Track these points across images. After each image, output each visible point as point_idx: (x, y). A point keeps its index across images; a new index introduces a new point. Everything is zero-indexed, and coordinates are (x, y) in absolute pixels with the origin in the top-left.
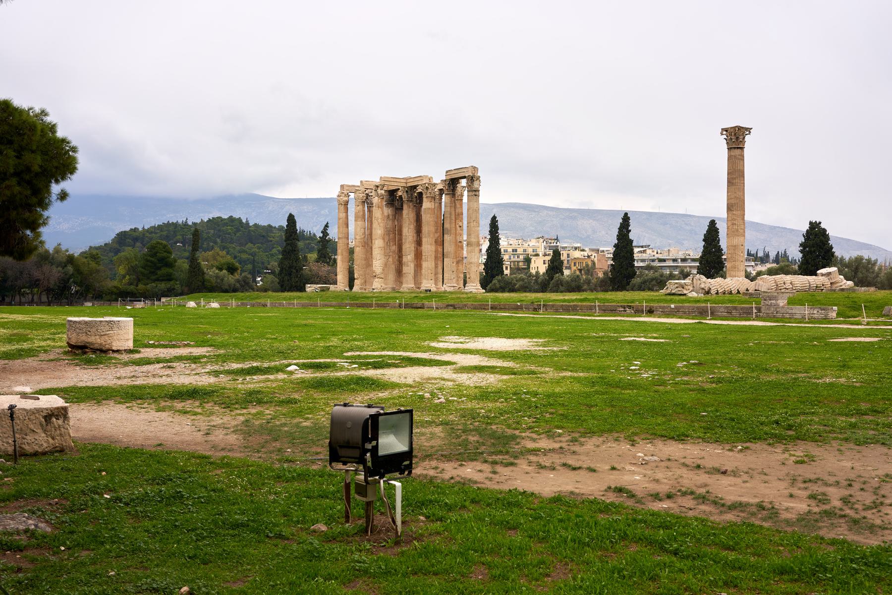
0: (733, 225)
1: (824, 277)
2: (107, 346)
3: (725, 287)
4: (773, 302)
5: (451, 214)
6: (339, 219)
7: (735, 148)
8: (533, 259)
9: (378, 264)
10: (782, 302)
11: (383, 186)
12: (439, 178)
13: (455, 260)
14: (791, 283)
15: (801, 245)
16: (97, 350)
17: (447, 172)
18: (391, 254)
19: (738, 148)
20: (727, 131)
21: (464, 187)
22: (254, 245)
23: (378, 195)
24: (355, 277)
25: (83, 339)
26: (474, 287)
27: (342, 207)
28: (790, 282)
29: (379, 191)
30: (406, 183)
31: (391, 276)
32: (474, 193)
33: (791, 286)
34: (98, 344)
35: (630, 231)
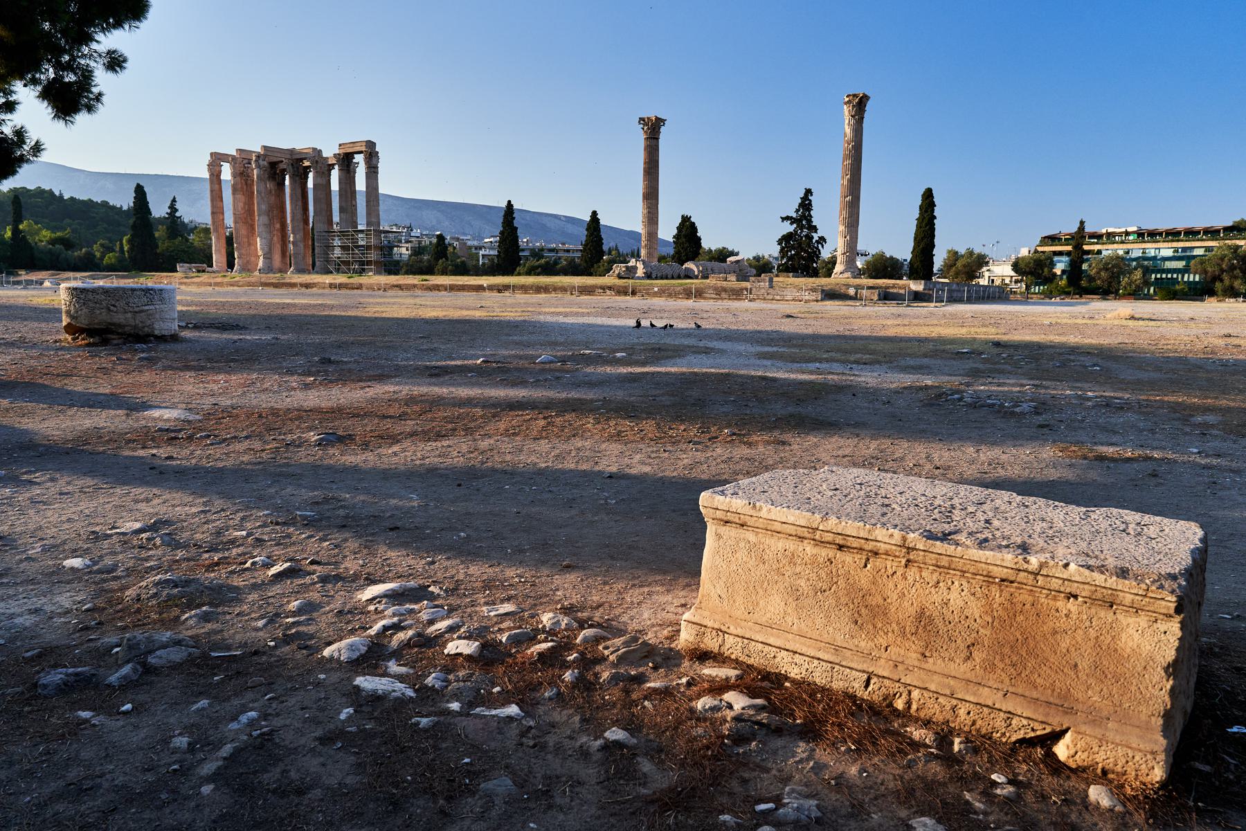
2: (146, 329)
6: (212, 191)
11: (265, 156)
12: (330, 151)
15: (674, 237)
16: (130, 335)
17: (340, 145)
18: (275, 233)
19: (654, 138)
21: (334, 165)
22: (74, 220)
25: (103, 317)
29: (261, 162)
32: (372, 171)
34: (130, 325)
35: (514, 218)
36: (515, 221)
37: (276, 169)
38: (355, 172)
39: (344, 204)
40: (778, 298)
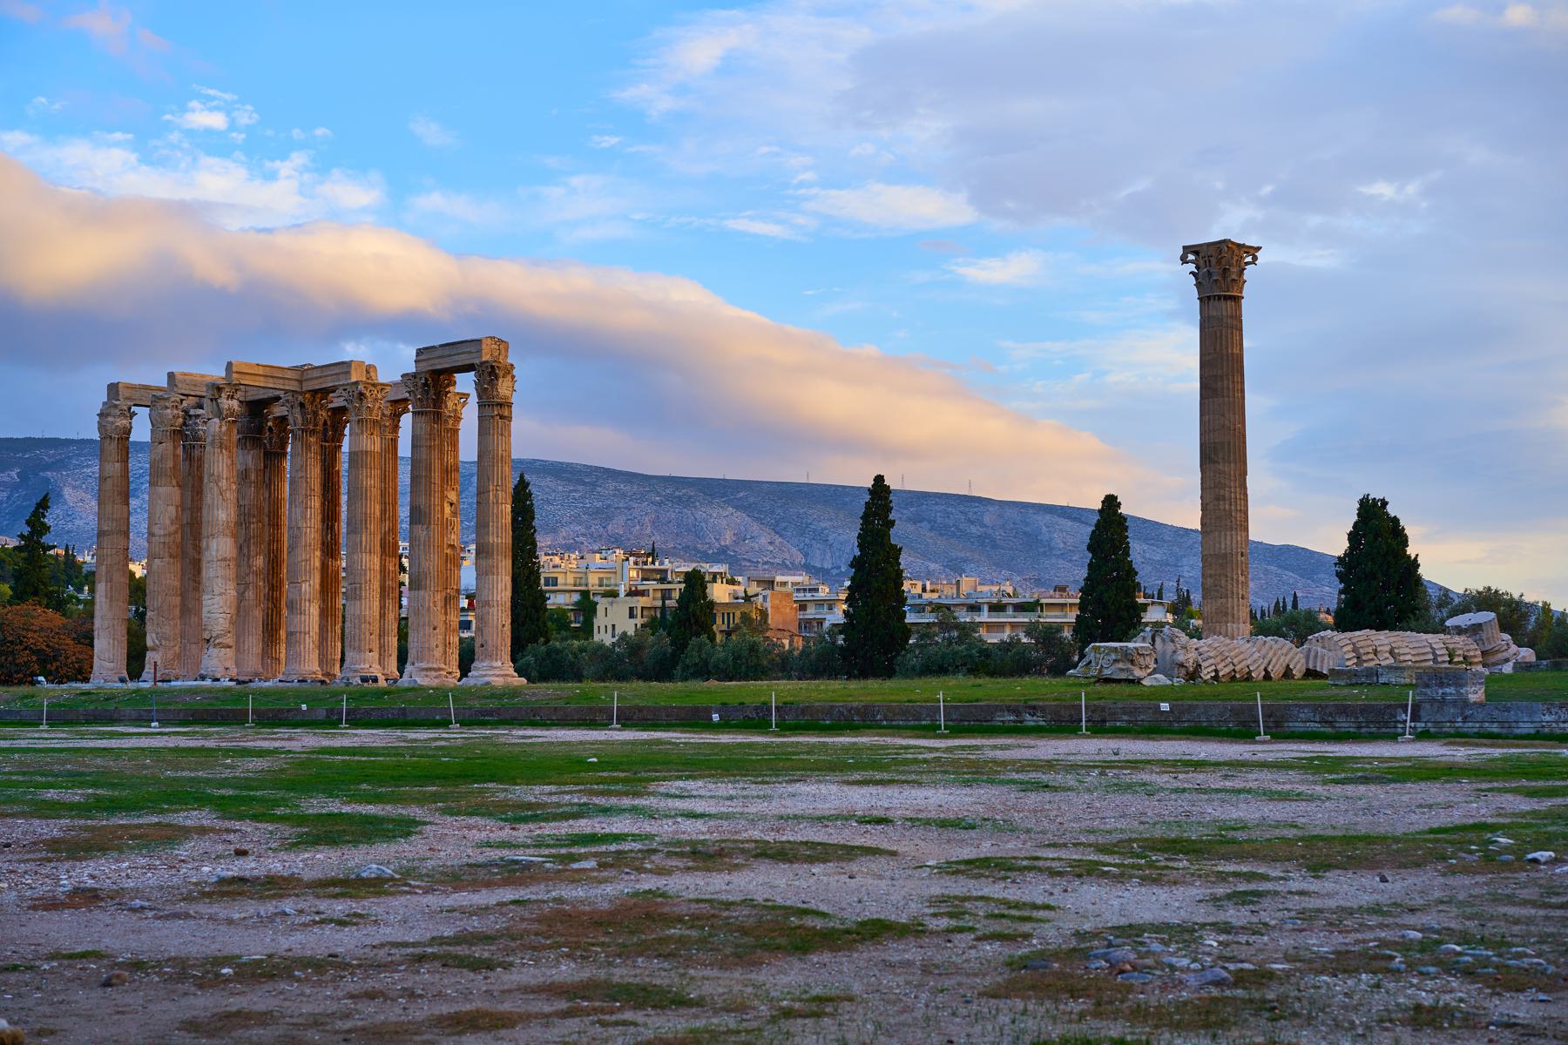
0: (1218, 499)
1: (1463, 637)
3: (1235, 661)
4: (1448, 690)
5: (429, 468)
7: (1219, 297)
8: (602, 604)
9: (218, 603)
10: (1476, 694)
11: (236, 387)
13: (439, 597)
14: (1391, 652)
18: (251, 578)
19: (1226, 298)
20: (1196, 253)
23: (219, 413)
24: (149, 643)
26: (497, 671)
27: (112, 447)
28: (1387, 648)
29: (225, 403)
30: (300, 382)
31: (254, 644)
32: (495, 410)
33: (1391, 661)
35: (892, 523)
36: (892, 531)
37: (265, 418)
38: (458, 419)
39: (422, 501)
40: (1495, 728)
